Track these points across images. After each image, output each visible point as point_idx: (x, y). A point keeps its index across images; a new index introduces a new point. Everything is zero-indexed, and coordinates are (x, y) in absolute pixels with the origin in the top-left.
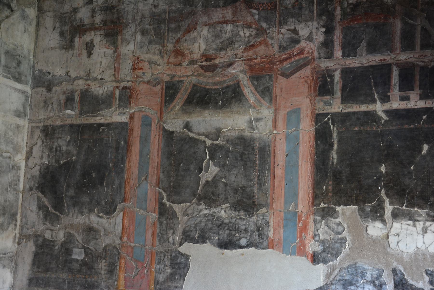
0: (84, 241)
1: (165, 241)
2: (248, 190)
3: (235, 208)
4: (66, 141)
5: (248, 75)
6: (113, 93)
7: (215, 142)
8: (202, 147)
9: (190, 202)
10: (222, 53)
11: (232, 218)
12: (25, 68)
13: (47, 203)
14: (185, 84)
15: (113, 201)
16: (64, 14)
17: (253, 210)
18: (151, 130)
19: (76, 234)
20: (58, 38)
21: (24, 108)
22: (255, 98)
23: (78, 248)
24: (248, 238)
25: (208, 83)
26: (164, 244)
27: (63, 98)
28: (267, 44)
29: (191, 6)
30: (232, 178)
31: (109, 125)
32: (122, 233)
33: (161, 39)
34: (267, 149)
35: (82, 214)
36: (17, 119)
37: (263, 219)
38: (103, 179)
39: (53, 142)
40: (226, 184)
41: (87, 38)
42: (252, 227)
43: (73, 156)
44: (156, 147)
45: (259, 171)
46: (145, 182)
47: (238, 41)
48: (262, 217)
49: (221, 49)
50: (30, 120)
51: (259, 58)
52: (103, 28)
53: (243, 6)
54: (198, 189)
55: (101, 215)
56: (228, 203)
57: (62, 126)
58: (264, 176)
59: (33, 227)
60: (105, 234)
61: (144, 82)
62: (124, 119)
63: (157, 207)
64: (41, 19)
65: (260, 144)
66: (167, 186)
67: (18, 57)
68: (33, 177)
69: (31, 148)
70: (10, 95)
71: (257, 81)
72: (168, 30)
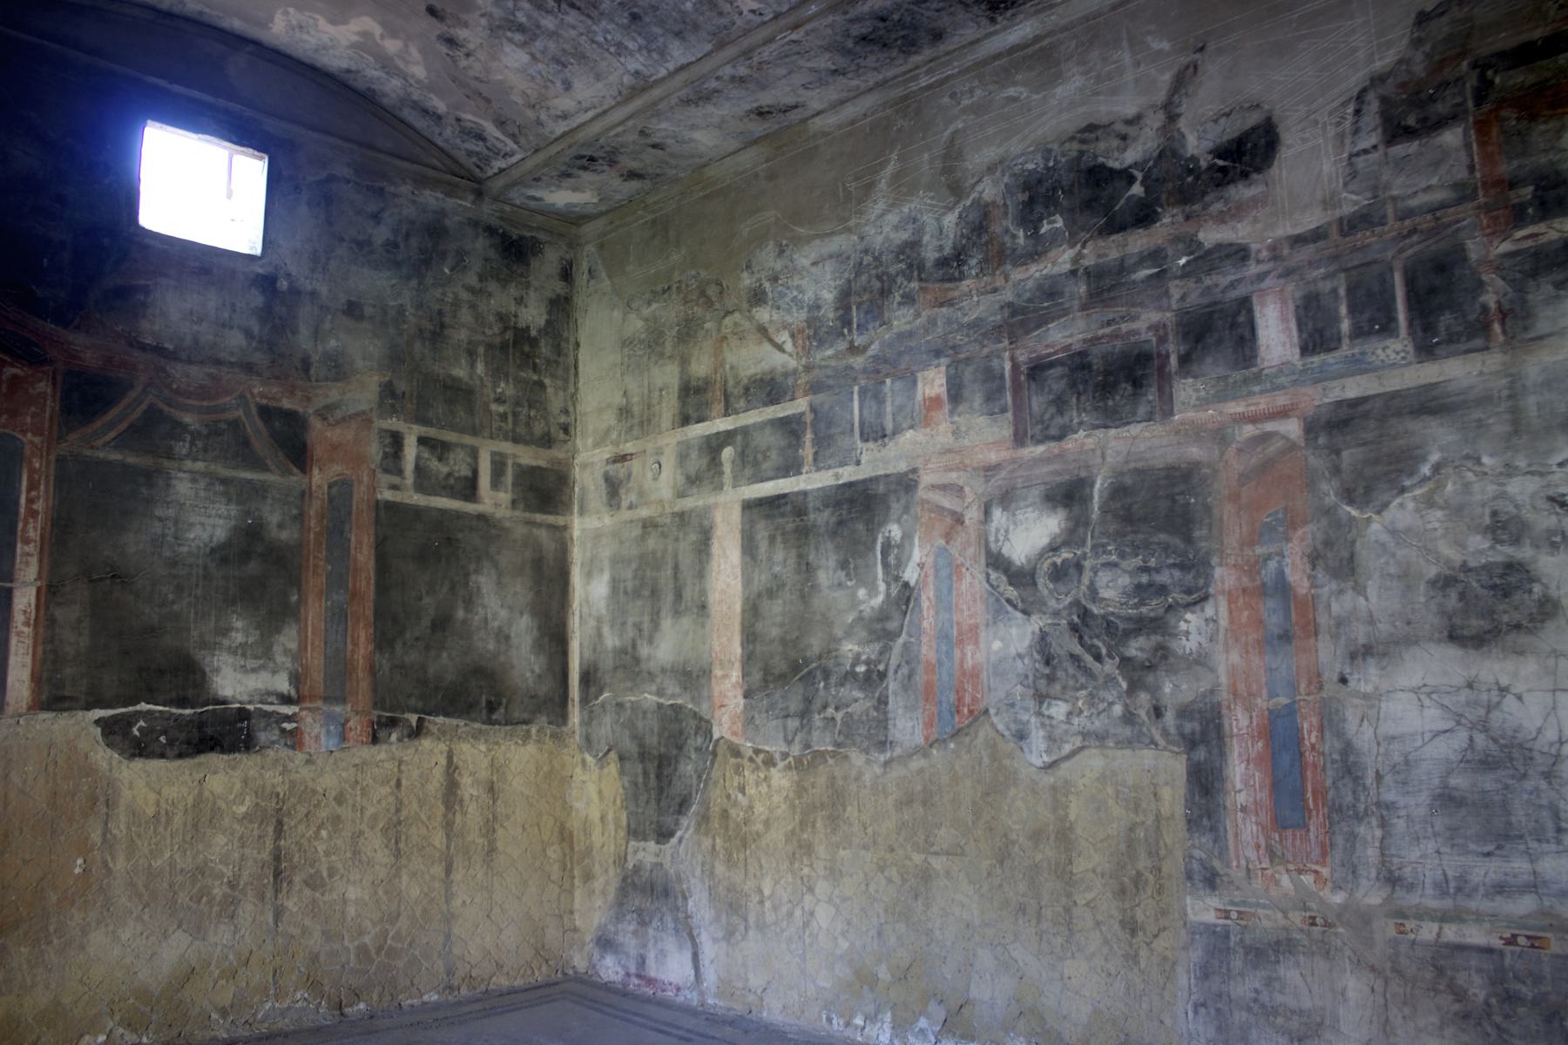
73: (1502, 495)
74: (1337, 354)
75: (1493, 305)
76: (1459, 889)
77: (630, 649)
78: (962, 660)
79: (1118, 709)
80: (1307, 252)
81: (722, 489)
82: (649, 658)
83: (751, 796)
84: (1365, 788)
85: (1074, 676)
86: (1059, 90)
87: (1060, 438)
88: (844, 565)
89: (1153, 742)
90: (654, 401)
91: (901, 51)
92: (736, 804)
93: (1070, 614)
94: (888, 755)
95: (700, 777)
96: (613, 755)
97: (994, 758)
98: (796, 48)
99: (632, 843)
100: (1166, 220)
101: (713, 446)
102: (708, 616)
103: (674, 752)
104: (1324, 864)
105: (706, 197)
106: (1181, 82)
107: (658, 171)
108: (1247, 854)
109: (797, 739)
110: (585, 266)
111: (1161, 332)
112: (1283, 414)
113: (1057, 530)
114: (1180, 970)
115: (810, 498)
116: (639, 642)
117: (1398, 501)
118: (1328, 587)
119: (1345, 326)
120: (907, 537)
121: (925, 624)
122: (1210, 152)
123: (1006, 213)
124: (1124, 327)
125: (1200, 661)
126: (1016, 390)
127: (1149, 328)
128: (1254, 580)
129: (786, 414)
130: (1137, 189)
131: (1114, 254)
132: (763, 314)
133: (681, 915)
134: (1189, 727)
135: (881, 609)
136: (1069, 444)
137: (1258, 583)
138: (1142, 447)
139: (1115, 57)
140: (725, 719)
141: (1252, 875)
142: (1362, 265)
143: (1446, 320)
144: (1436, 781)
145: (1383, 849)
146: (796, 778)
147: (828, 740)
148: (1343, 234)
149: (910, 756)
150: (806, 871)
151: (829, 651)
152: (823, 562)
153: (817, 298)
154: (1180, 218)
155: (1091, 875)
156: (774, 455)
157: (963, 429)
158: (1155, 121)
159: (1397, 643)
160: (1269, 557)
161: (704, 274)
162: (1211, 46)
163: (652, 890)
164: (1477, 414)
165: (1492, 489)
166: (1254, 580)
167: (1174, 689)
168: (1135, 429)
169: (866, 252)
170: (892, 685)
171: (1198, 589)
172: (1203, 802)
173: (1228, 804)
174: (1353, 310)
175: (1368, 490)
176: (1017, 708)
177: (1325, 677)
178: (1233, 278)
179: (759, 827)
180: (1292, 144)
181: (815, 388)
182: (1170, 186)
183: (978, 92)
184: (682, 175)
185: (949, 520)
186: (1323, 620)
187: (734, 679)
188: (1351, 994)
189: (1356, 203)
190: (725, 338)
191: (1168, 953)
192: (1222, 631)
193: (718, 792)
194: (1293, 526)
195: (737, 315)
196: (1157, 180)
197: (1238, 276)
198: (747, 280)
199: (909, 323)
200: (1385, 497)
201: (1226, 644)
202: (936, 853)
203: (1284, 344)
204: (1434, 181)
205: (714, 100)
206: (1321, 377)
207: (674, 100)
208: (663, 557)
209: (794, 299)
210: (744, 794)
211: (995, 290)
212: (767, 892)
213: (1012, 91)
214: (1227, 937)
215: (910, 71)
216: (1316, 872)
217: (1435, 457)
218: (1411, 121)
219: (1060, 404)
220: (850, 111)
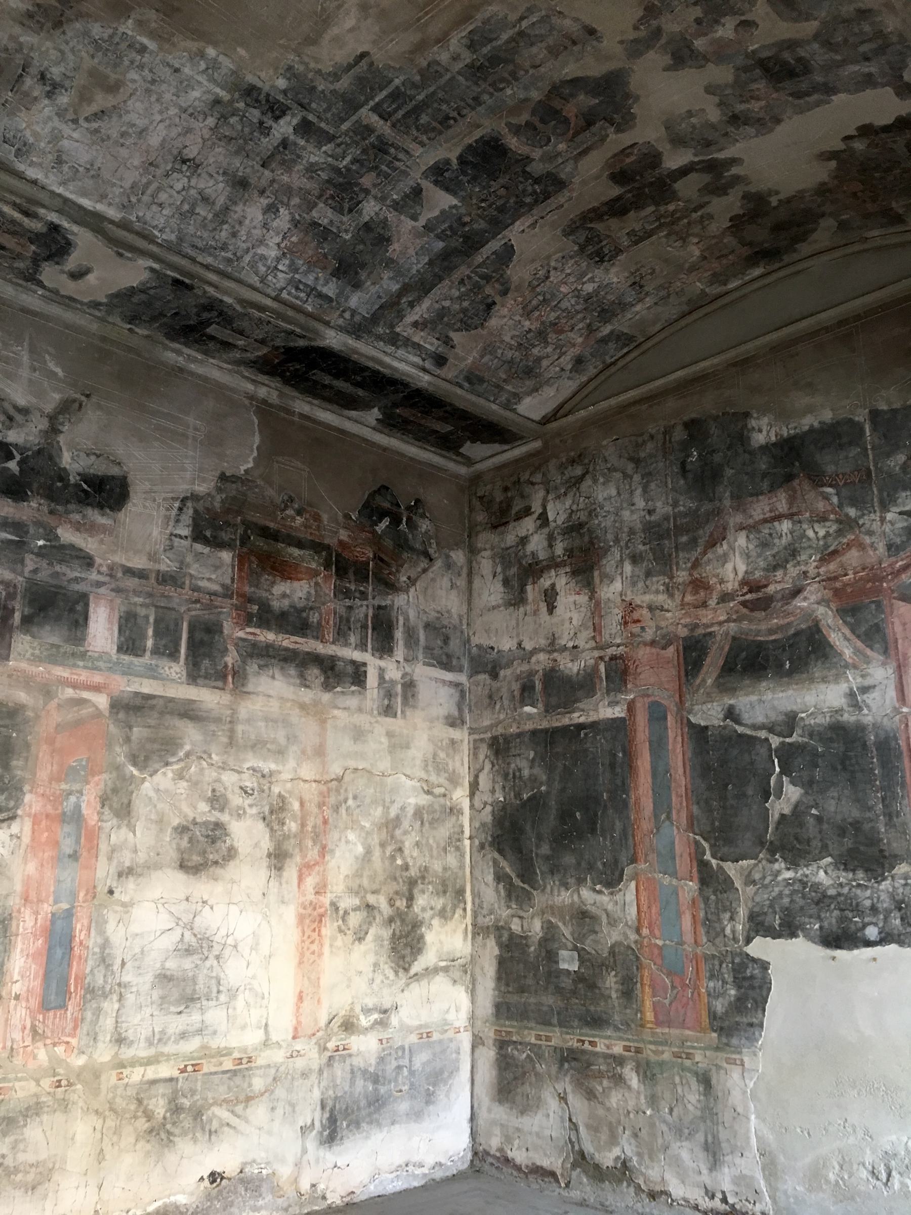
0: (576, 935)
1: (717, 935)
2: (867, 827)
3: (845, 864)
4: (527, 759)
5: (833, 606)
6: (595, 668)
7: (788, 740)
8: (763, 751)
9: (756, 858)
10: (777, 574)
11: (841, 885)
12: (455, 644)
13: (508, 870)
14: (718, 638)
15: (616, 861)
16: (507, 549)
17: (883, 867)
18: (666, 728)
19: (560, 924)
20: (502, 589)
21: (460, 710)
22: (855, 648)
23: (567, 949)
24: (881, 925)
25: (759, 631)
26: (718, 941)
27: (516, 687)
28: (862, 547)
29: (711, 501)
30: (831, 805)
31: (594, 725)
32: (639, 920)
33: (666, 564)
34: (893, 744)
35: (566, 886)
36: (451, 730)
37: (906, 884)
38: (595, 823)
39: (509, 764)
40: (819, 819)
41: (545, 582)
42: (886, 903)
43: (541, 784)
44: (680, 757)
45: (882, 788)
46: (667, 823)
47: (805, 548)
48: (902, 882)
49: (775, 568)
50: (471, 728)
51: (850, 572)
52: (569, 561)
53: (806, 486)
54: (767, 832)
55: (598, 887)
56: (831, 855)
57: (519, 735)
58: (894, 798)
59: (491, 912)
60: (609, 923)
61: (645, 644)
62: (618, 712)
63: (695, 870)
64: (474, 564)
65: (876, 736)
66: (709, 829)
68: (483, 825)
69: (477, 777)
71: (853, 616)
72: (676, 548)
73: (218, 780)
74: (141, 660)
75: (230, 665)
76: (160, 1040)
80: (132, 583)
84: (113, 973)
100: (34, 504)
104: (73, 1035)
106: (67, 408)
108: (14, 1036)
111: (11, 590)
112: (97, 688)
118: (111, 821)
119: (150, 643)
122: (79, 474)
128: (56, 809)
137: (59, 811)
139: (15, 349)
141: (14, 1053)
143: (206, 662)
144: (158, 965)
145: (117, 1017)
154: (45, 509)
159: (149, 868)
160: (70, 793)
162: (94, 399)
164: (213, 727)
166: (56, 809)
171: (8, 810)
174: (156, 634)
175: (147, 758)
177: (99, 889)
178: (78, 575)
180: (136, 504)
182: (42, 480)
186: (104, 847)
188: (78, 1137)
196: (33, 469)
200: (157, 766)
203: (107, 639)
204: (213, 577)
206: (128, 672)
216: (68, 1043)
217: (187, 747)
218: (208, 534)
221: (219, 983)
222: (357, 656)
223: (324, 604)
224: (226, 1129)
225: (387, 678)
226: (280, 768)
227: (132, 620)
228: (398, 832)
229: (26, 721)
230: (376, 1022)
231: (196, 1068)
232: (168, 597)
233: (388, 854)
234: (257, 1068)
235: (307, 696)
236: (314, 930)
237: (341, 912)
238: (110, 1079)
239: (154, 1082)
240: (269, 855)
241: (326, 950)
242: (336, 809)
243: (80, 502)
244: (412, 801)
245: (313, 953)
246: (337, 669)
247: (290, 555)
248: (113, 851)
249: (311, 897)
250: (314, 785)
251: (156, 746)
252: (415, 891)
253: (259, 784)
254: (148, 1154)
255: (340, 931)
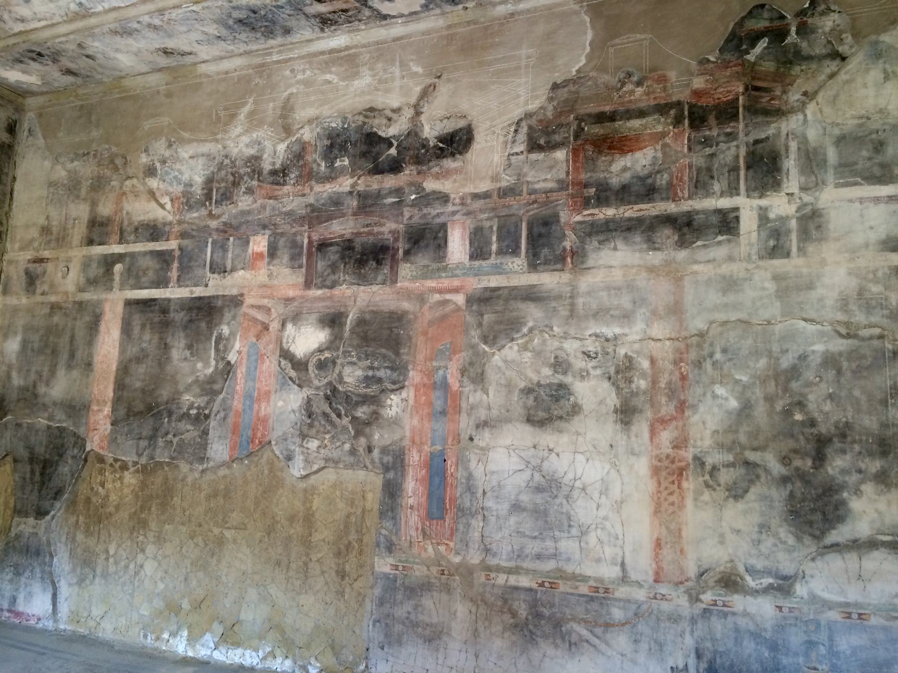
67: (874, 136)
70: (862, 216)
73: (561, 348)
74: (488, 262)
75: (568, 248)
76: (519, 556)
77: (31, 388)
78: (258, 413)
79: (347, 446)
80: (478, 204)
81: (111, 290)
82: (45, 394)
83: (108, 489)
85: (324, 426)
86: (356, 82)
87: (331, 287)
88: (190, 347)
89: (365, 466)
90: (69, 226)
91: (263, 35)
92: (97, 493)
93: (326, 389)
94: (205, 466)
95: (73, 475)
96: (9, 459)
97: (271, 470)
98: (194, 16)
99: (16, 519)
100: (407, 172)
101: (109, 262)
102: (92, 371)
103: (56, 458)
104: (451, 540)
105: (121, 98)
106: (425, 94)
107: (89, 74)
109: (145, 453)
110: (26, 126)
111: (396, 235)
112: (456, 290)
113: (324, 340)
114: (367, 600)
115: (172, 303)
116: (39, 384)
117: (509, 345)
118: (468, 388)
119: (494, 247)
120: (233, 334)
121: (238, 388)
123: (316, 151)
124: (376, 229)
125: (396, 422)
126: (310, 255)
127: (390, 232)
129: (162, 248)
130: (393, 151)
131: (375, 186)
132: (153, 183)
133: (47, 569)
134: (388, 459)
135: (211, 376)
136: (337, 292)
138: (377, 299)
139: (391, 70)
140: (96, 438)
142: (507, 216)
143: (545, 251)
144: (513, 497)
146: (141, 478)
147: (166, 454)
148: (500, 197)
149: (219, 467)
150: (141, 538)
151: (174, 399)
152: (176, 344)
153: (191, 180)
155: (322, 543)
156: (151, 273)
157: (275, 274)
158: (408, 113)
159: (500, 421)
160: (439, 368)
161: (114, 149)
162: (444, 77)
163: (27, 551)
164: (554, 304)
165: (556, 344)
167: (379, 437)
168: (375, 288)
169: (226, 157)
170: (213, 423)
171: (399, 382)
172: (390, 502)
173: (403, 504)
174: (499, 239)
176: (289, 441)
177: (462, 436)
178: (439, 211)
179: (112, 509)
181: (183, 235)
183: (308, 73)
184: (106, 80)
185: (260, 327)
186: (464, 405)
187: (106, 413)
188: (459, 614)
189: (508, 181)
190: (124, 194)
191: (362, 591)
192: (410, 406)
193: (85, 486)
194: (454, 352)
195: (135, 181)
196: (405, 148)
197: (442, 211)
198: (144, 159)
199: (249, 205)
200: (503, 342)
201: (411, 414)
202: (229, 528)
204: (549, 177)
205: (134, 36)
206: (478, 273)
207: (106, 29)
208: (63, 329)
209: (175, 177)
210: (103, 488)
211: (304, 195)
212: (112, 552)
213: (328, 77)
214: (396, 581)
215: (267, 49)
216: (447, 544)
217: (530, 324)
218: (542, 142)
219: (334, 268)
220: (226, 65)
221: (569, 519)
222: (725, 203)
223: (675, 163)
224: (585, 644)
225: (772, 216)
226: (627, 331)
227: (479, 233)
228: (794, 385)
229: (409, 322)
230: (770, 588)
231: (553, 586)
232: (509, 206)
233: (778, 408)
234: (615, 599)
235: (655, 258)
236: (673, 482)
237: (708, 468)
238: (480, 577)
239: (516, 588)
240: (616, 411)
241: (689, 502)
242: (698, 364)
243: (437, 158)
244: (819, 348)
245: (673, 504)
246: (695, 223)
247: (630, 129)
248: (472, 408)
249: (667, 449)
250: (668, 343)
251: (502, 327)
252: (829, 451)
253: (603, 348)
254: (514, 643)
255: (707, 486)
